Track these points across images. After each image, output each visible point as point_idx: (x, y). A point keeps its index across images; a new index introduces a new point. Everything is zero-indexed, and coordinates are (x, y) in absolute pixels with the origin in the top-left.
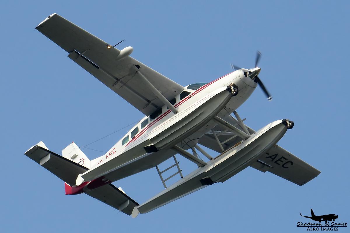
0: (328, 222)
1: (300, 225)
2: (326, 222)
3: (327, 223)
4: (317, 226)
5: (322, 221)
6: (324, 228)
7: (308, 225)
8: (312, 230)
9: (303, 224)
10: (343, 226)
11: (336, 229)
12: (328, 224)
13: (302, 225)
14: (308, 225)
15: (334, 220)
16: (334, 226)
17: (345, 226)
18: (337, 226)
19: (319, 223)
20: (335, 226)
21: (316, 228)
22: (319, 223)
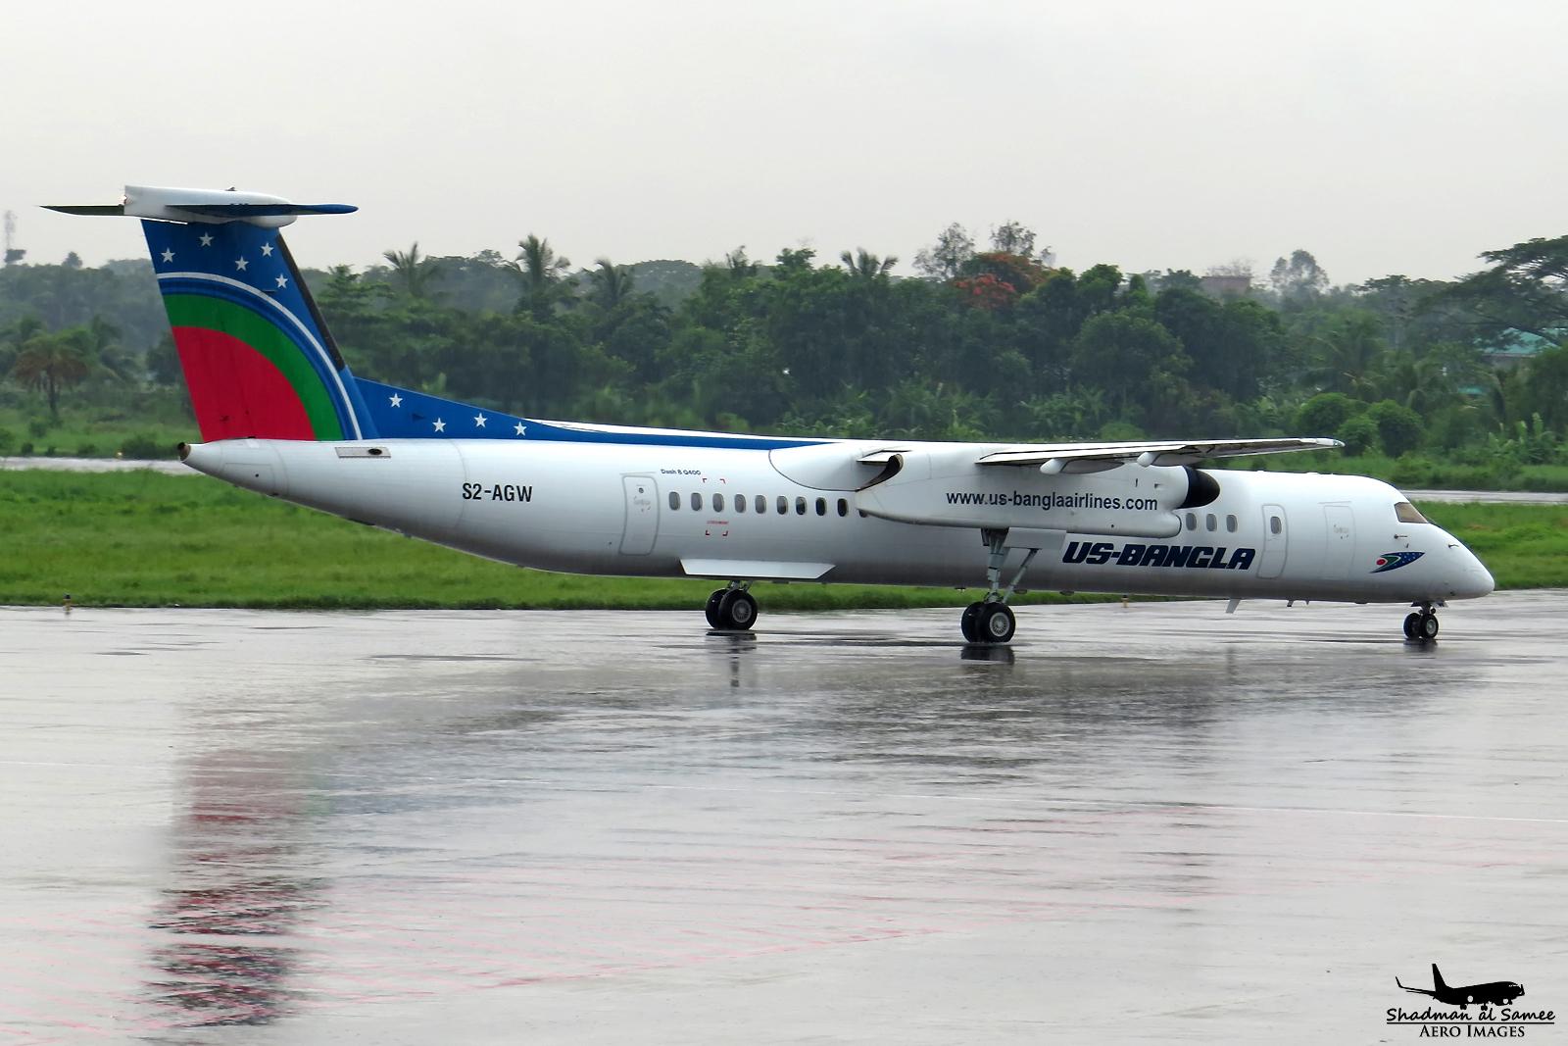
0: (1489, 1009)
1: (1395, 1017)
2: (1484, 1008)
3: (1487, 1013)
4: (1453, 1021)
5: (1469, 1006)
6: (1476, 1030)
7: (1422, 1017)
8: (1436, 1034)
9: (1405, 1014)
10: (1539, 1020)
11: (1517, 1030)
12: (1490, 1015)
13: (1403, 1020)
14: (1422, 1017)
15: (1510, 1003)
16: (1510, 1020)
17: (1547, 1020)
18: (1521, 1020)
19: (1460, 1012)
20: (1515, 1021)
21: (1449, 1027)
22: (1459, 1013)
